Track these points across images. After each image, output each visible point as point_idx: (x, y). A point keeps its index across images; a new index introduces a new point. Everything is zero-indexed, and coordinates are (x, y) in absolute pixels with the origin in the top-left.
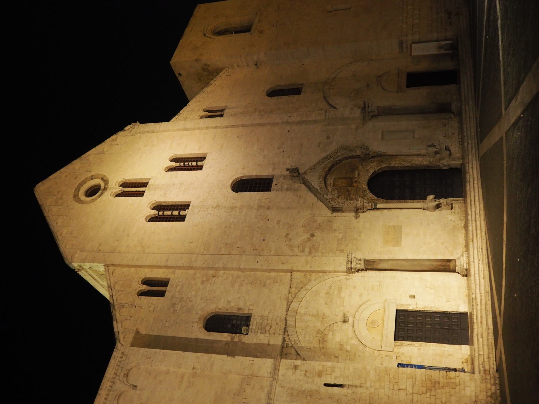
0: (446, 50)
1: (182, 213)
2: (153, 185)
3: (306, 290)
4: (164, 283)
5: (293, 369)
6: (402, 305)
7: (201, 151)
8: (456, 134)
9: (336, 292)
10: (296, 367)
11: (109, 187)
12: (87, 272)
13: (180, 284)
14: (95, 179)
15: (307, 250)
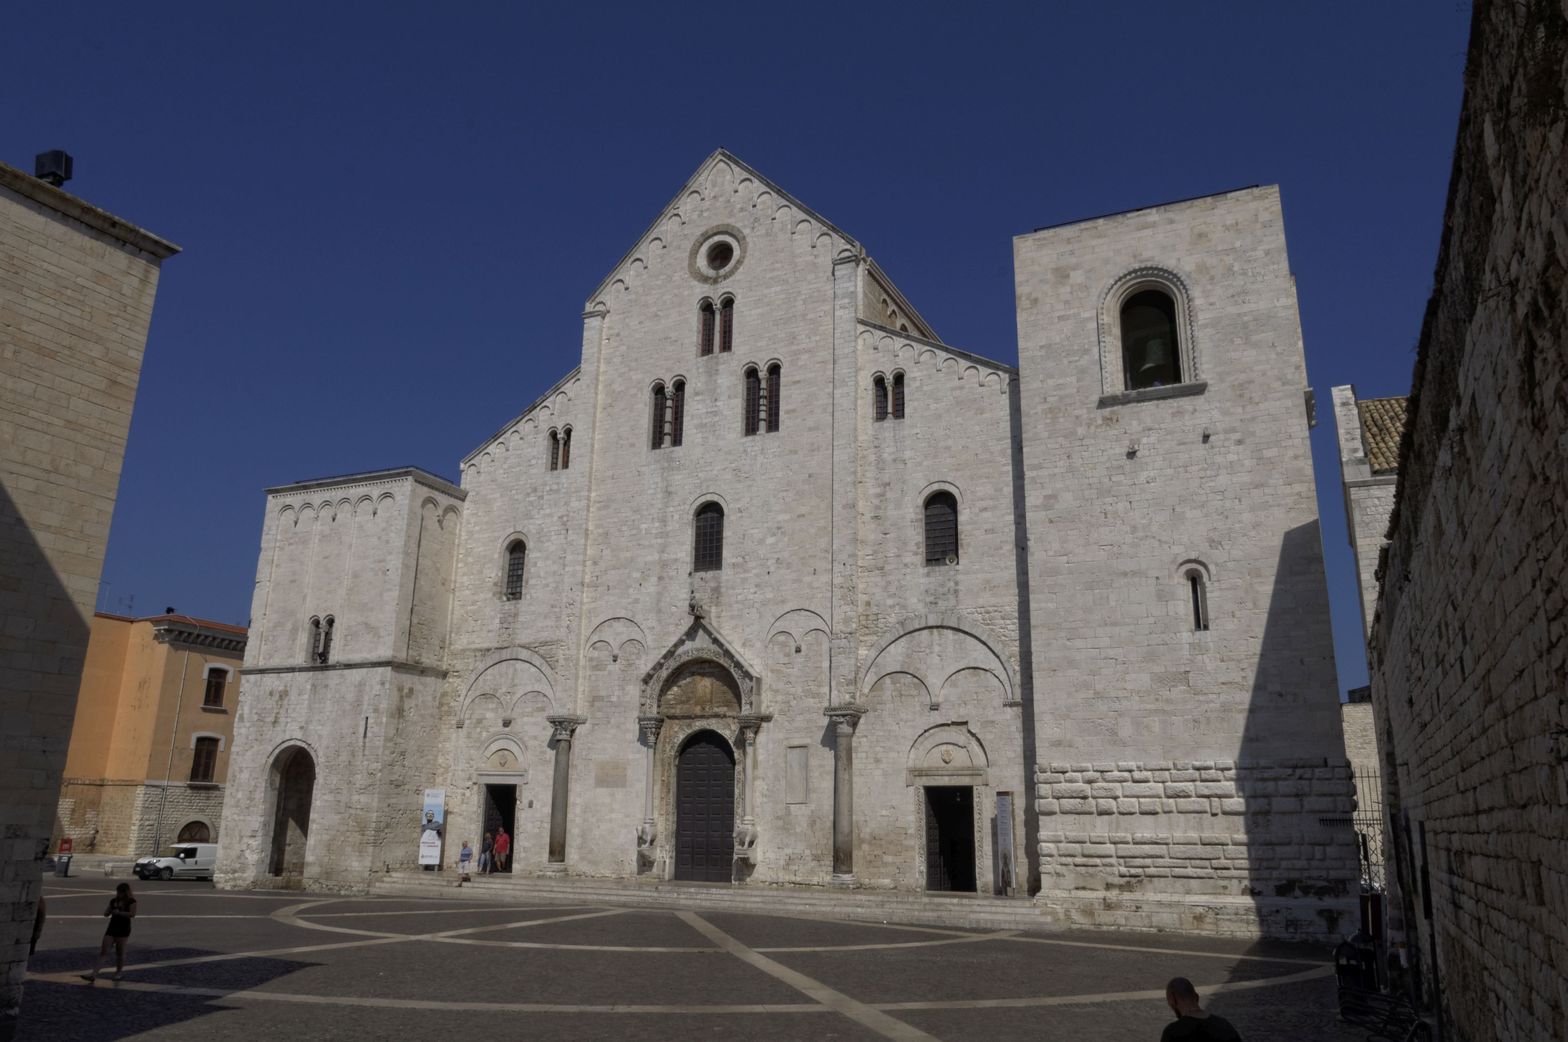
0: (1003, 871)
2: (717, 363)
6: (521, 791)
8: (793, 879)
9: (540, 705)
10: (383, 684)
13: (560, 486)
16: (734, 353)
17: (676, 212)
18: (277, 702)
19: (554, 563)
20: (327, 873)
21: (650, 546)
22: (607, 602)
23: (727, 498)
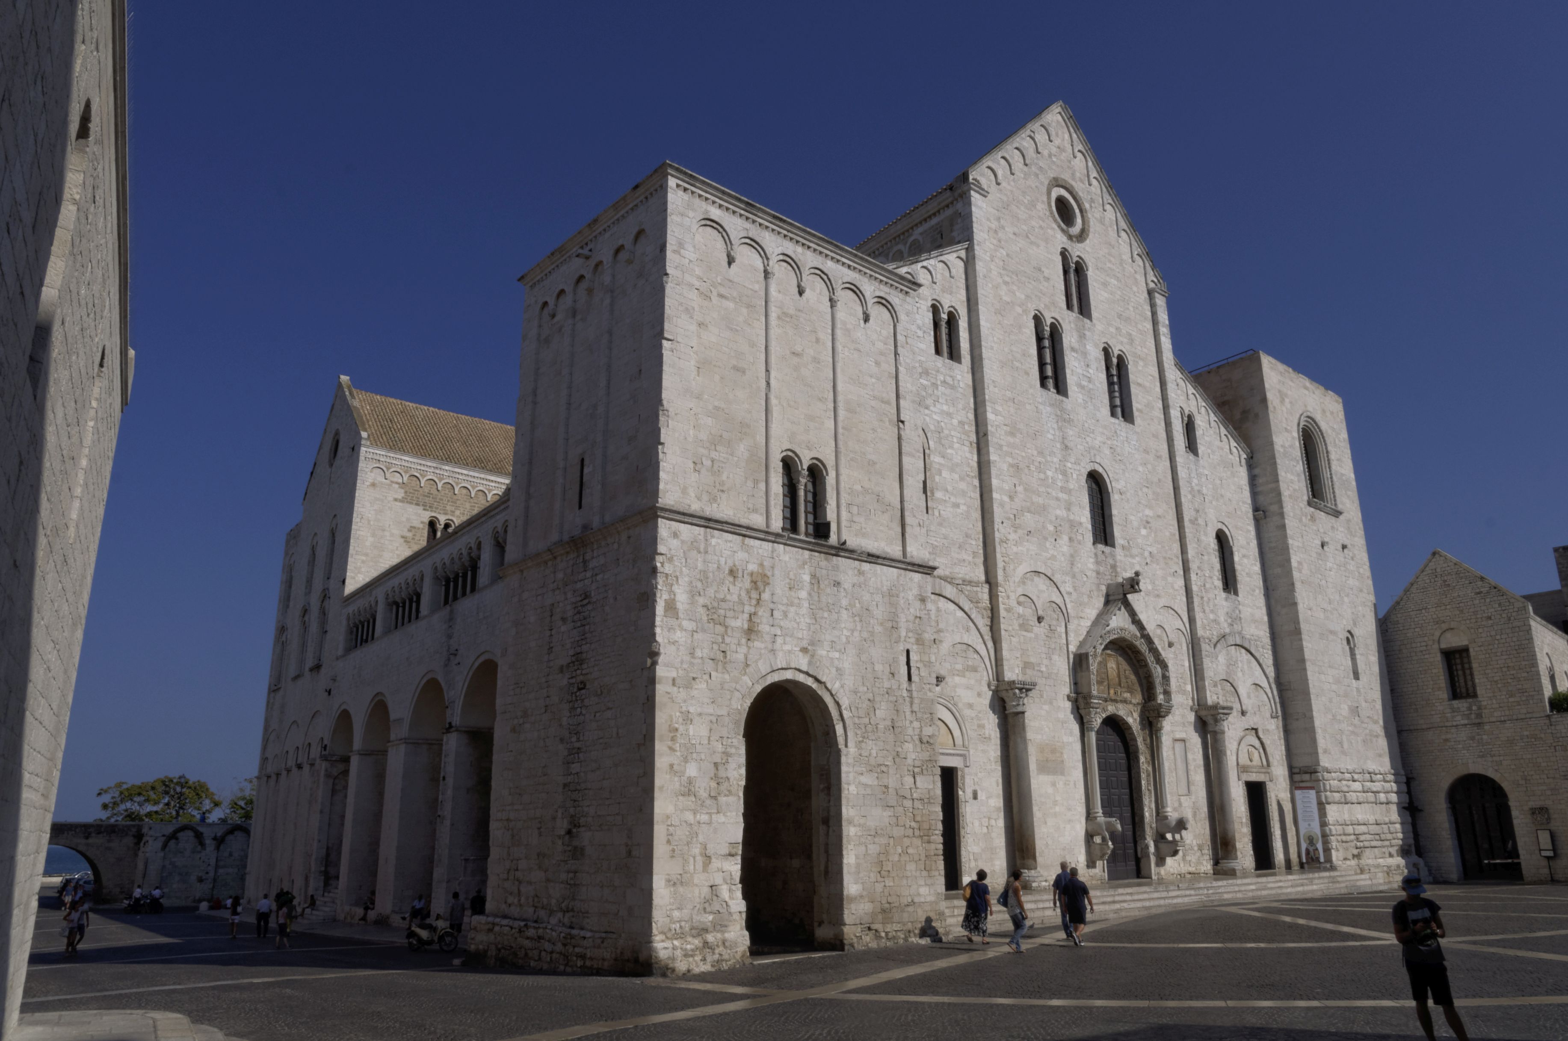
1: (1050, 383)
2: (1084, 326)
3: (971, 609)
4: (954, 355)
5: (920, 595)
6: (963, 777)
7: (1136, 413)
9: (970, 663)
10: (923, 600)
11: (1074, 245)
12: (947, 206)
13: (956, 382)
14: (1082, 216)
15: (1020, 610)
16: (1094, 325)
17: (1032, 134)
18: (748, 592)
19: (962, 479)
20: (883, 911)
21: (1058, 499)
22: (1028, 550)
23: (1111, 475)
